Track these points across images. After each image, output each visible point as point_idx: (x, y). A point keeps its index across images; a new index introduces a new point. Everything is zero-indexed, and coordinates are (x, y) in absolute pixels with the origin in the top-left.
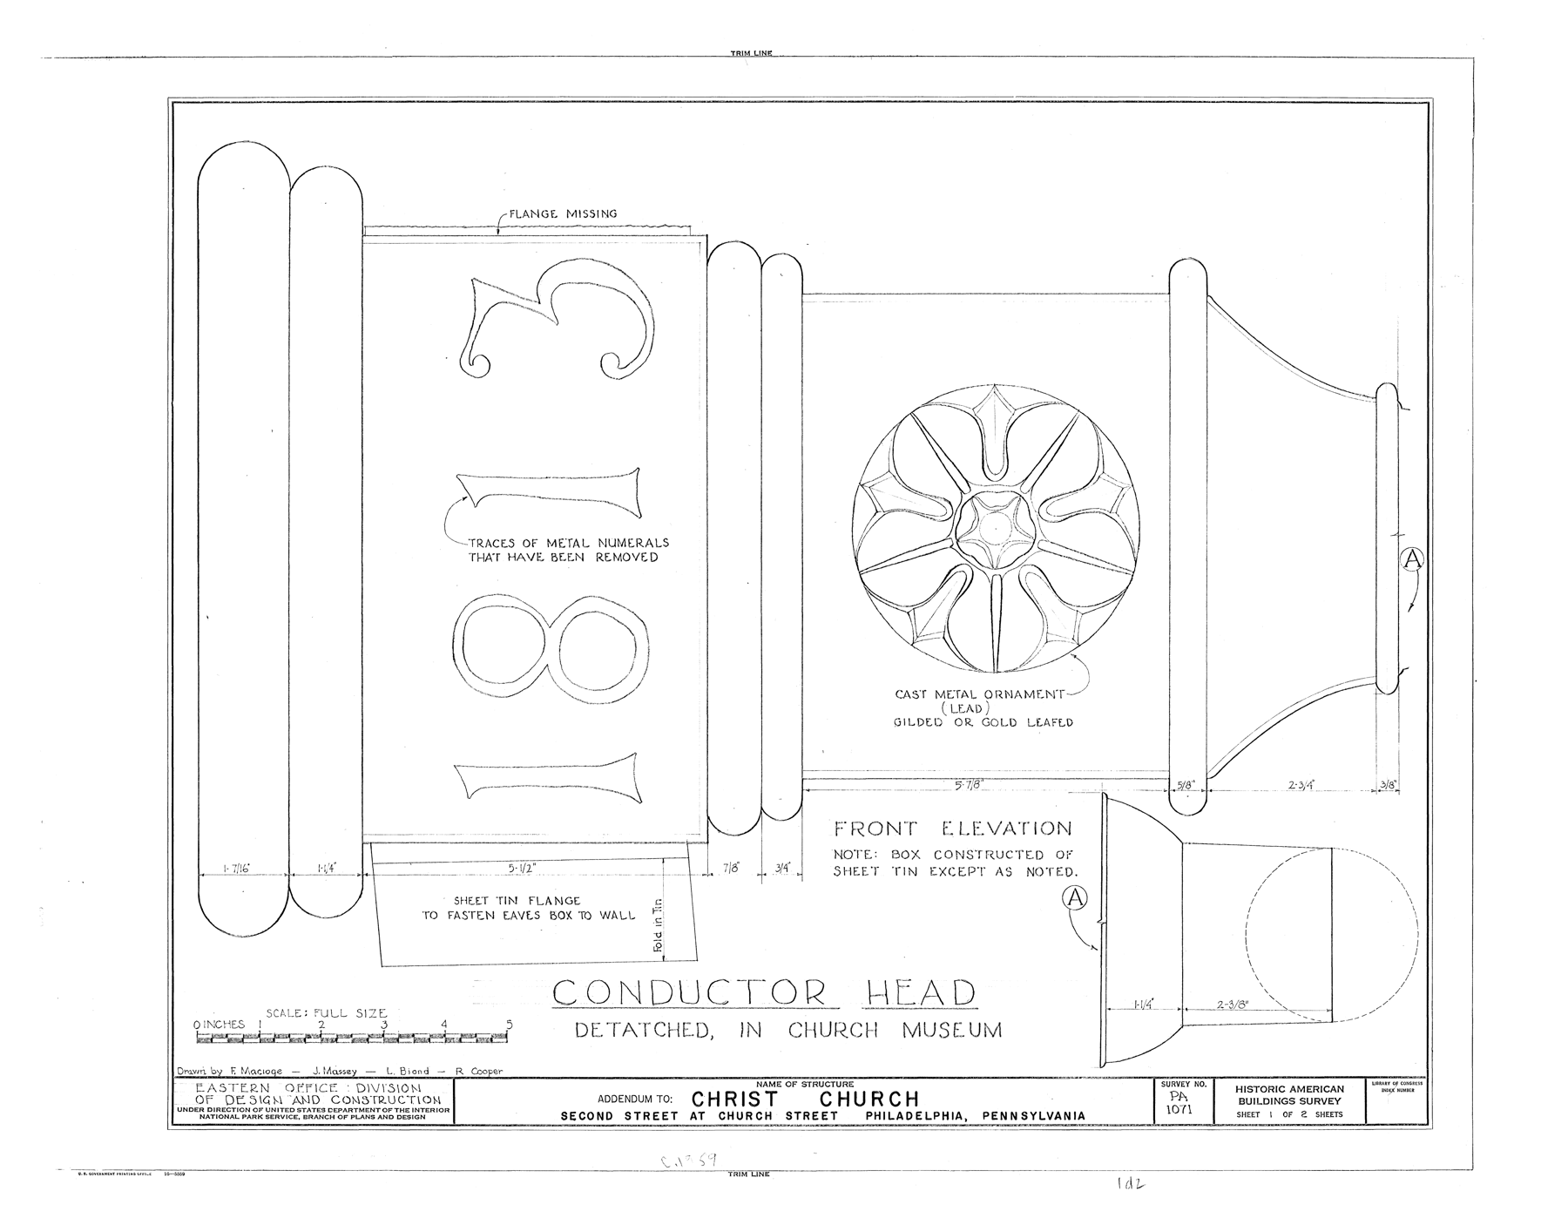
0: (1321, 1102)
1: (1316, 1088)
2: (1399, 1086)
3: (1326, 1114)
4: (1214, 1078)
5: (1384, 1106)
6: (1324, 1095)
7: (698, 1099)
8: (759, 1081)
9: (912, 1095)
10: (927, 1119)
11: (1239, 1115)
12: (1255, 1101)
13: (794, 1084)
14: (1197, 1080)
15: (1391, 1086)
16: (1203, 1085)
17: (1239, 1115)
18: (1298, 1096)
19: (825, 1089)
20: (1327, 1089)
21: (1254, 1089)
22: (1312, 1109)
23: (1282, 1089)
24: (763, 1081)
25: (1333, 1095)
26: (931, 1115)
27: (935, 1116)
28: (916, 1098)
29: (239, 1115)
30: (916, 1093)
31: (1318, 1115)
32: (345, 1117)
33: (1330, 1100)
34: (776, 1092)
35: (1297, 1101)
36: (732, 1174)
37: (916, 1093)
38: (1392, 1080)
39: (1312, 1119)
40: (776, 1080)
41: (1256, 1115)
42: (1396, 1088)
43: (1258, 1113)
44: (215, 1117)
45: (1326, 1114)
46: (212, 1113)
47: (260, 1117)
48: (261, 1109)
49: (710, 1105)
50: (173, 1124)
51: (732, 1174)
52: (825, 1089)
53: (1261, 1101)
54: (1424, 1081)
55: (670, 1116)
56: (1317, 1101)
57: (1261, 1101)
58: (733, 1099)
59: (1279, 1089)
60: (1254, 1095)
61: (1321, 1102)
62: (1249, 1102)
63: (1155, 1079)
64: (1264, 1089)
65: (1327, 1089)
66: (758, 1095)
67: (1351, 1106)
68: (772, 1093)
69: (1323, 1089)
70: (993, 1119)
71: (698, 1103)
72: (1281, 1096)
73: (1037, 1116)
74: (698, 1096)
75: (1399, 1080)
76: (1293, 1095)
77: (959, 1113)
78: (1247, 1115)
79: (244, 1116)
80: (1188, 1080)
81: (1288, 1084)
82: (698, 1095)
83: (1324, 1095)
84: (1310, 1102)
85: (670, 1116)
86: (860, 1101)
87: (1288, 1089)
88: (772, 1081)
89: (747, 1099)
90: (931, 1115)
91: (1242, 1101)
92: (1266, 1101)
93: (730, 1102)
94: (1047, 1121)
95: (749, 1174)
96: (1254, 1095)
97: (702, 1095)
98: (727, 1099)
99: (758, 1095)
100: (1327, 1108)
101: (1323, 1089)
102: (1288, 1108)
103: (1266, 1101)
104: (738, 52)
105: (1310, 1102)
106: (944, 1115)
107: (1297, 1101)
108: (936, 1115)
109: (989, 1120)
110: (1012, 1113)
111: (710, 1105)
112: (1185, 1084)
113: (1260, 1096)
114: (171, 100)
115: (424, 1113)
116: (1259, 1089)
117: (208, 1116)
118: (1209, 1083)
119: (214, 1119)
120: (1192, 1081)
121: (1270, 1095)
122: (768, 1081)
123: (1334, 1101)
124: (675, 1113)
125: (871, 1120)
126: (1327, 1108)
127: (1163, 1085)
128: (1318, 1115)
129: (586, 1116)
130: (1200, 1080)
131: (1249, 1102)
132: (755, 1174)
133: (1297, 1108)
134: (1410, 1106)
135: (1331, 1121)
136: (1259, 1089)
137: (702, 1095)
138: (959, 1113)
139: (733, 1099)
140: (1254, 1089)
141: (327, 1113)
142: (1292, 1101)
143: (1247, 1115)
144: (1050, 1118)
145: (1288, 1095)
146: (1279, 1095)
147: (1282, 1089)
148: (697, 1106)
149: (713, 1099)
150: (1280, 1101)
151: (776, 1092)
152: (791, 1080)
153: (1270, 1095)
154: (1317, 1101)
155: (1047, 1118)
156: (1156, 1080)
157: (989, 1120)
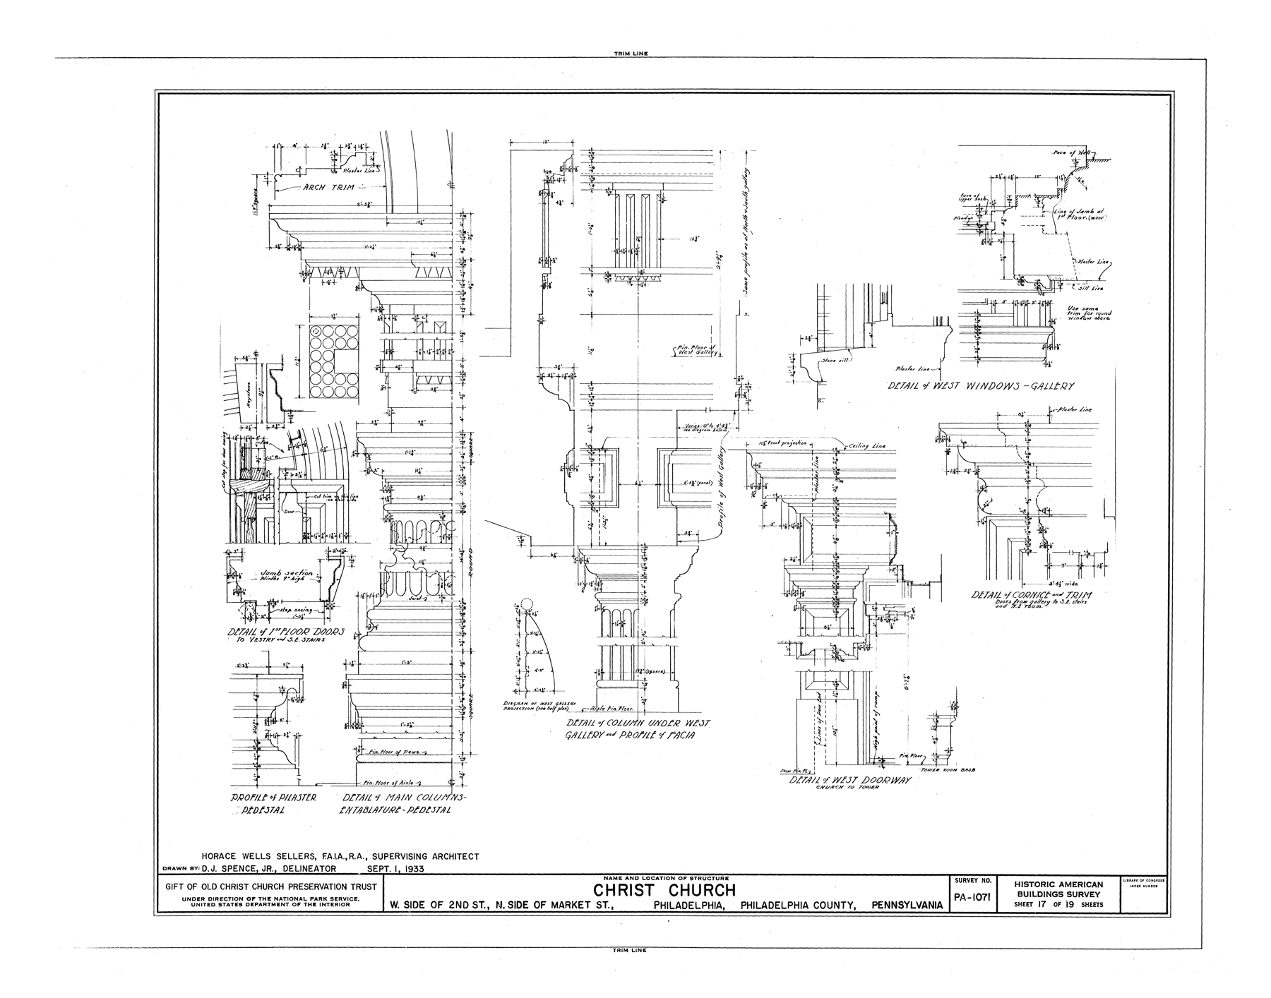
0: (1084, 895)
1: (1080, 884)
2: (1145, 883)
3: (1090, 905)
4: (997, 875)
5: (1137, 898)
6: (1087, 890)
7: (599, 890)
8: (606, 876)
9: (1017, 886)
10: (912, 908)
11: (1017, 904)
12: (1031, 894)
13: (685, 878)
14: (984, 877)
15: (1138, 883)
16: (989, 881)
17: (1017, 904)
18: (1065, 890)
19: (672, 882)
20: (1089, 885)
21: (1030, 884)
22: (1078, 901)
23: (1052, 884)
24: (609, 876)
25: (1094, 889)
26: (785, 905)
27: (789, 905)
28: (734, 890)
29: (217, 903)
30: (734, 885)
31: (1084, 905)
32: (299, 904)
33: (1091, 894)
34: (653, 885)
35: (1065, 894)
36: (616, 950)
37: (734, 885)
38: (1139, 878)
39: (1078, 908)
40: (618, 876)
41: (1029, 904)
42: (1142, 884)
43: (1031, 903)
44: (234, 905)
45: (1090, 905)
46: (212, 902)
47: (241, 905)
48: (253, 898)
49: (607, 895)
50: (158, 912)
51: (616, 950)
52: (672, 882)
53: (1036, 894)
54: (1165, 878)
55: (584, 905)
56: (1081, 894)
57: (1036, 894)
58: (625, 890)
59: (1051, 884)
60: (1029, 889)
61: (1084, 895)
62: (1026, 895)
63: (950, 875)
64: (1037, 884)
65: (1089, 885)
66: (642, 886)
67: (1108, 896)
68: (650, 885)
69: (1086, 884)
70: (879, 908)
71: (599, 893)
72: (1052, 890)
73: (909, 905)
74: (599, 887)
75: (1145, 878)
76: (1062, 889)
77: (806, 903)
78: (1023, 904)
79: (220, 905)
80: (976, 877)
81: (1057, 880)
82: (599, 887)
83: (1087, 890)
84: (1075, 895)
85: (584, 905)
86: (697, 892)
87: (1057, 884)
88: (615, 876)
89: (634, 890)
90: (785, 905)
91: (1020, 894)
92: (1040, 894)
93: (708, 892)
94: (917, 910)
95: (630, 950)
96: (1029, 889)
97: (602, 887)
98: (620, 890)
99: (642, 886)
100: (1089, 900)
101: (1086, 884)
102: (1058, 899)
103: (1040, 894)
104: (620, 53)
105: (1075, 895)
106: (795, 905)
107: (1065, 894)
108: (790, 904)
109: (876, 909)
110: (835, 903)
111: (607, 895)
112: (974, 881)
113: (1036, 890)
114: (1172, 93)
115: (349, 902)
116: (1033, 884)
117: (208, 904)
118: (993, 879)
119: (200, 907)
120: (980, 878)
121: (1043, 889)
122: (612, 876)
123: (1095, 895)
124: (588, 902)
125: (745, 909)
126: (1089, 900)
127: (957, 881)
128: (1084, 905)
129: (819, 905)
130: (986, 877)
131: (1026, 895)
132: (634, 950)
133: (1065, 899)
134: (1152, 898)
135: (1095, 911)
136: (1033, 884)
137: (602, 887)
138: (806, 903)
139: (625, 890)
140: (1030, 884)
141: (343, 901)
142: (1061, 894)
143: (1023, 904)
144: (919, 907)
145: (1057, 889)
146: (1049, 889)
147: (1052, 884)
148: (674, 895)
149: (610, 890)
150: (1051, 894)
151: (653, 885)
152: (683, 876)
153: (1043, 889)
154: (1081, 894)
155: (917, 907)
156: (952, 877)
157: (876, 909)
